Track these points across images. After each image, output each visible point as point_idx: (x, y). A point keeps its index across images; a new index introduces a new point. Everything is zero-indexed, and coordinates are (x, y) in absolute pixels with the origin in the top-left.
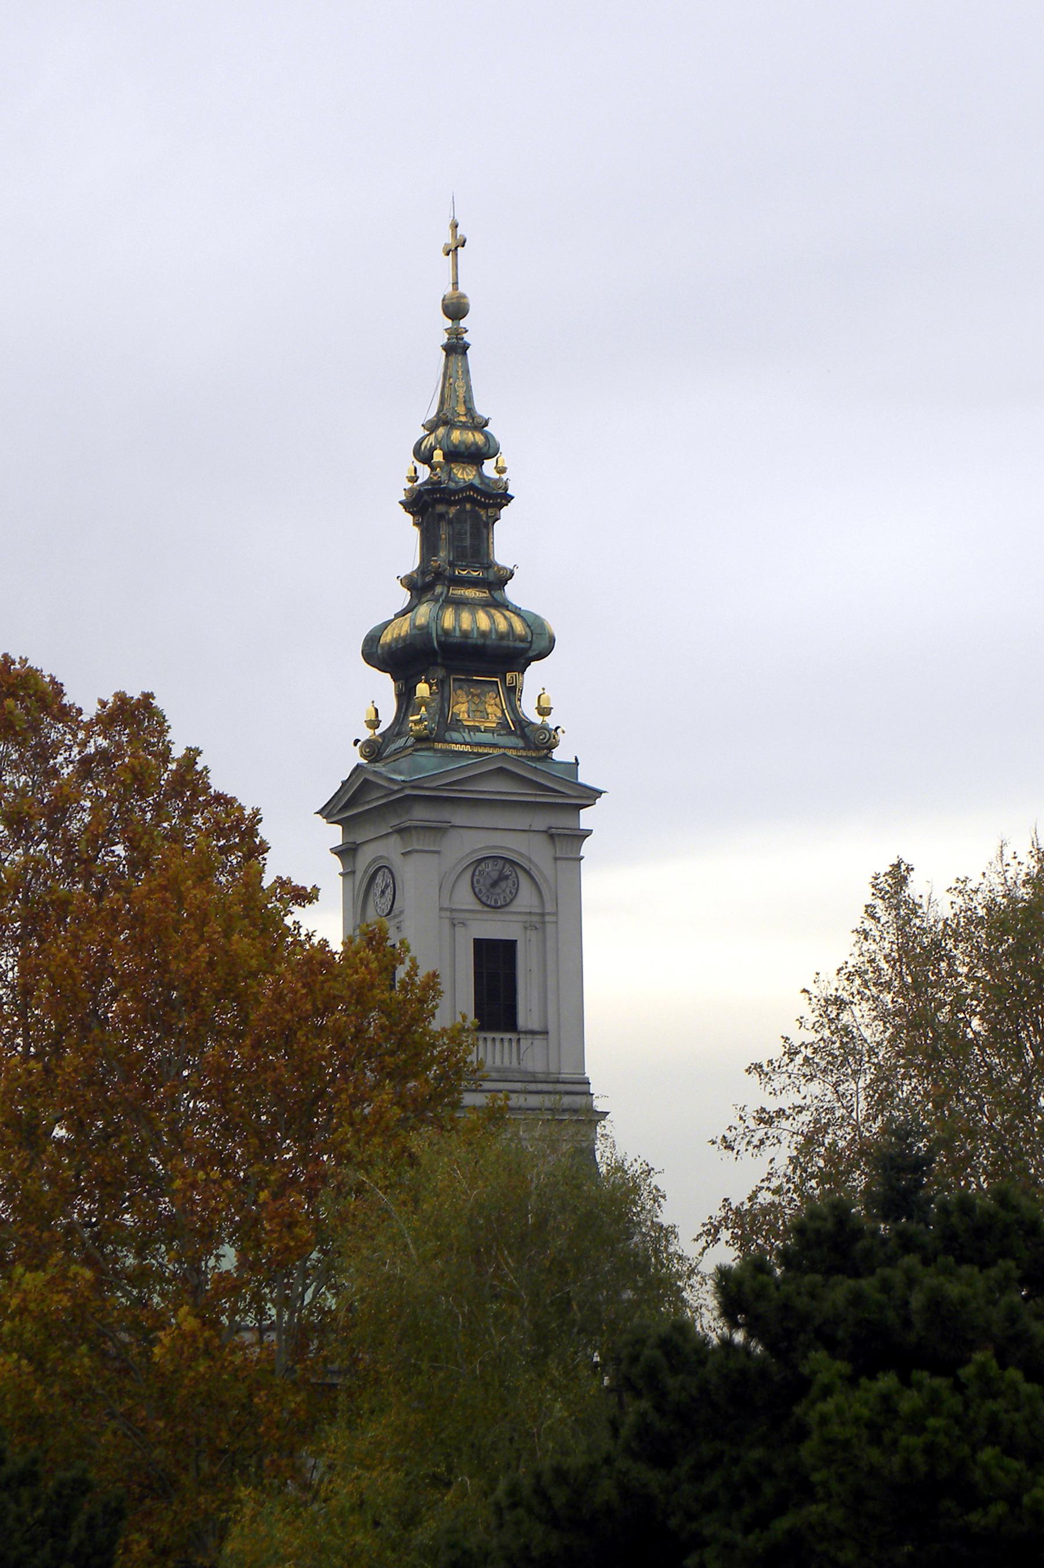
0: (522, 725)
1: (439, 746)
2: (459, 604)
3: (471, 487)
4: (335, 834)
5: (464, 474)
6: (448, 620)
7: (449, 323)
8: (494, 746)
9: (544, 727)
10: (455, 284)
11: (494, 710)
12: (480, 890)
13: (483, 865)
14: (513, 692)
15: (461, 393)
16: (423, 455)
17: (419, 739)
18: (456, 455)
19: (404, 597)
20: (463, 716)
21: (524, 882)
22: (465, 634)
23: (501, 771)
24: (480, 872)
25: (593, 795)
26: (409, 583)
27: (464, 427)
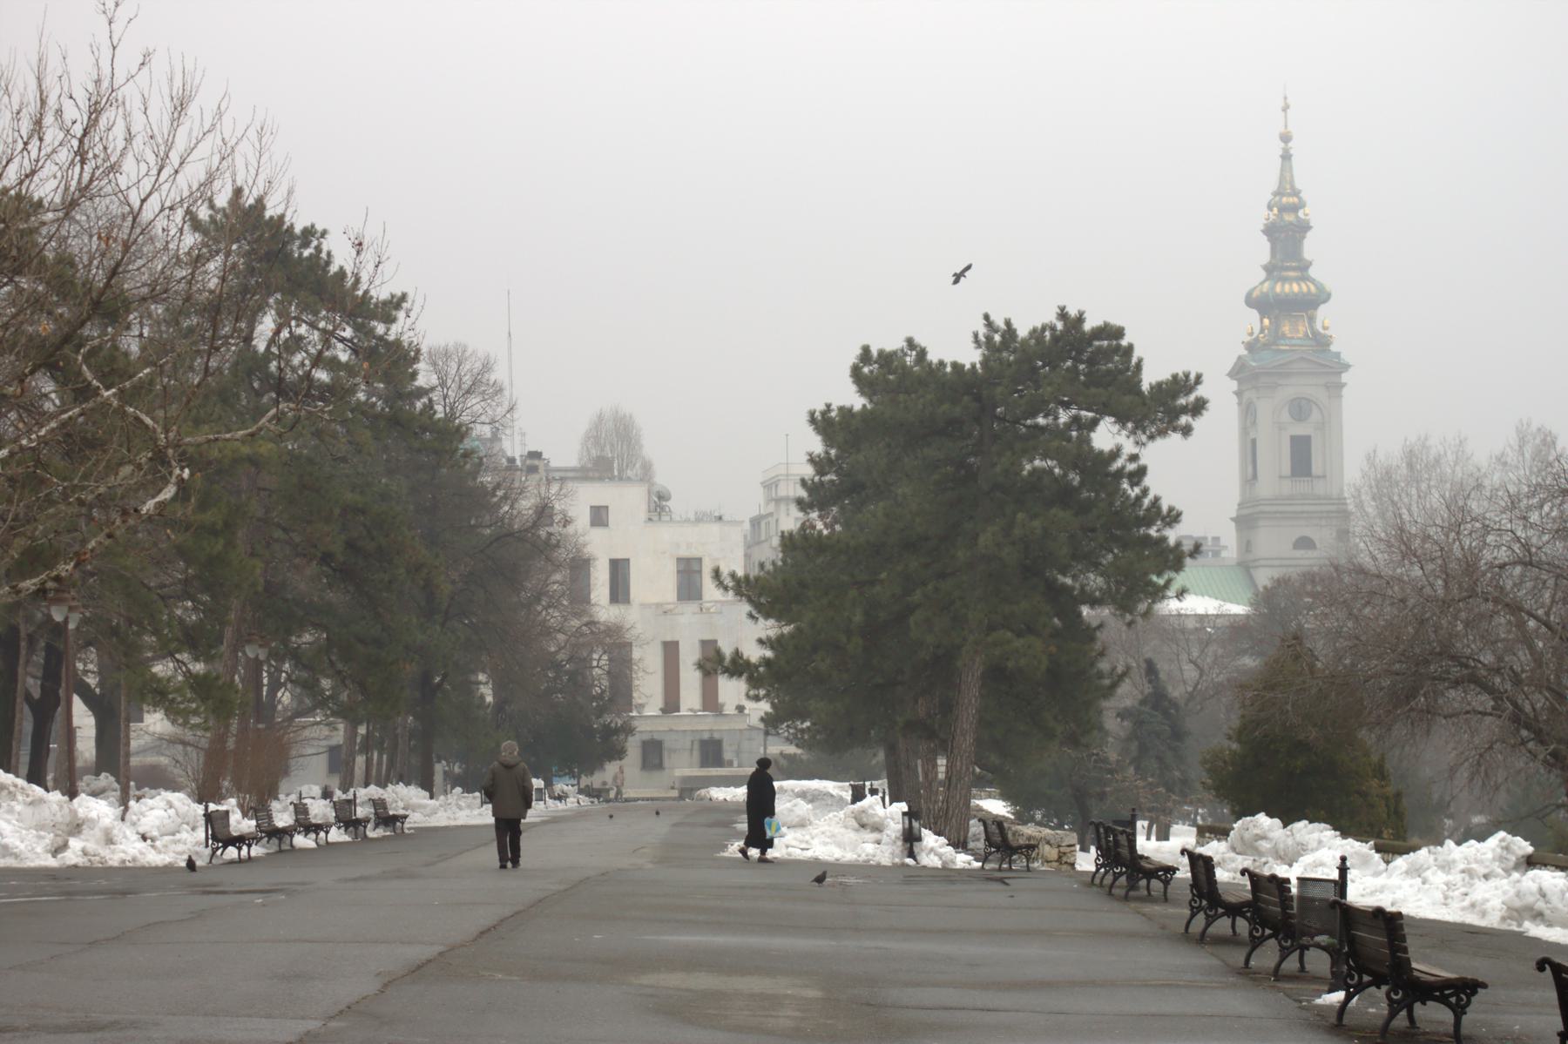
0: (1316, 334)
1: (1273, 347)
2: (1284, 280)
3: (1291, 223)
4: (1234, 385)
5: (1289, 218)
6: (1278, 289)
7: (1282, 145)
8: (1302, 346)
9: (1324, 336)
10: (1286, 126)
11: (1302, 328)
14: (1312, 319)
15: (1288, 179)
16: (1270, 208)
17: (1265, 345)
18: (1283, 209)
19: (1263, 275)
20: (1287, 332)
21: (1314, 407)
22: (1287, 295)
23: (1302, 359)
25: (1346, 367)
26: (1266, 268)
27: (1289, 195)
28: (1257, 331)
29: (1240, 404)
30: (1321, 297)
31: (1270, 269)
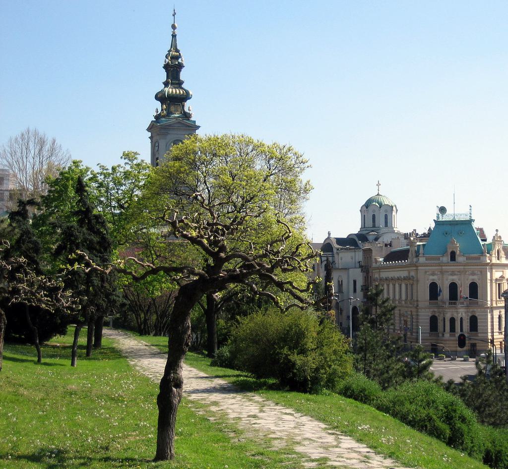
4: (149, 134)
14: (183, 106)
25: (198, 127)
28: (160, 111)
29: (152, 142)
30: (186, 97)
31: (166, 84)
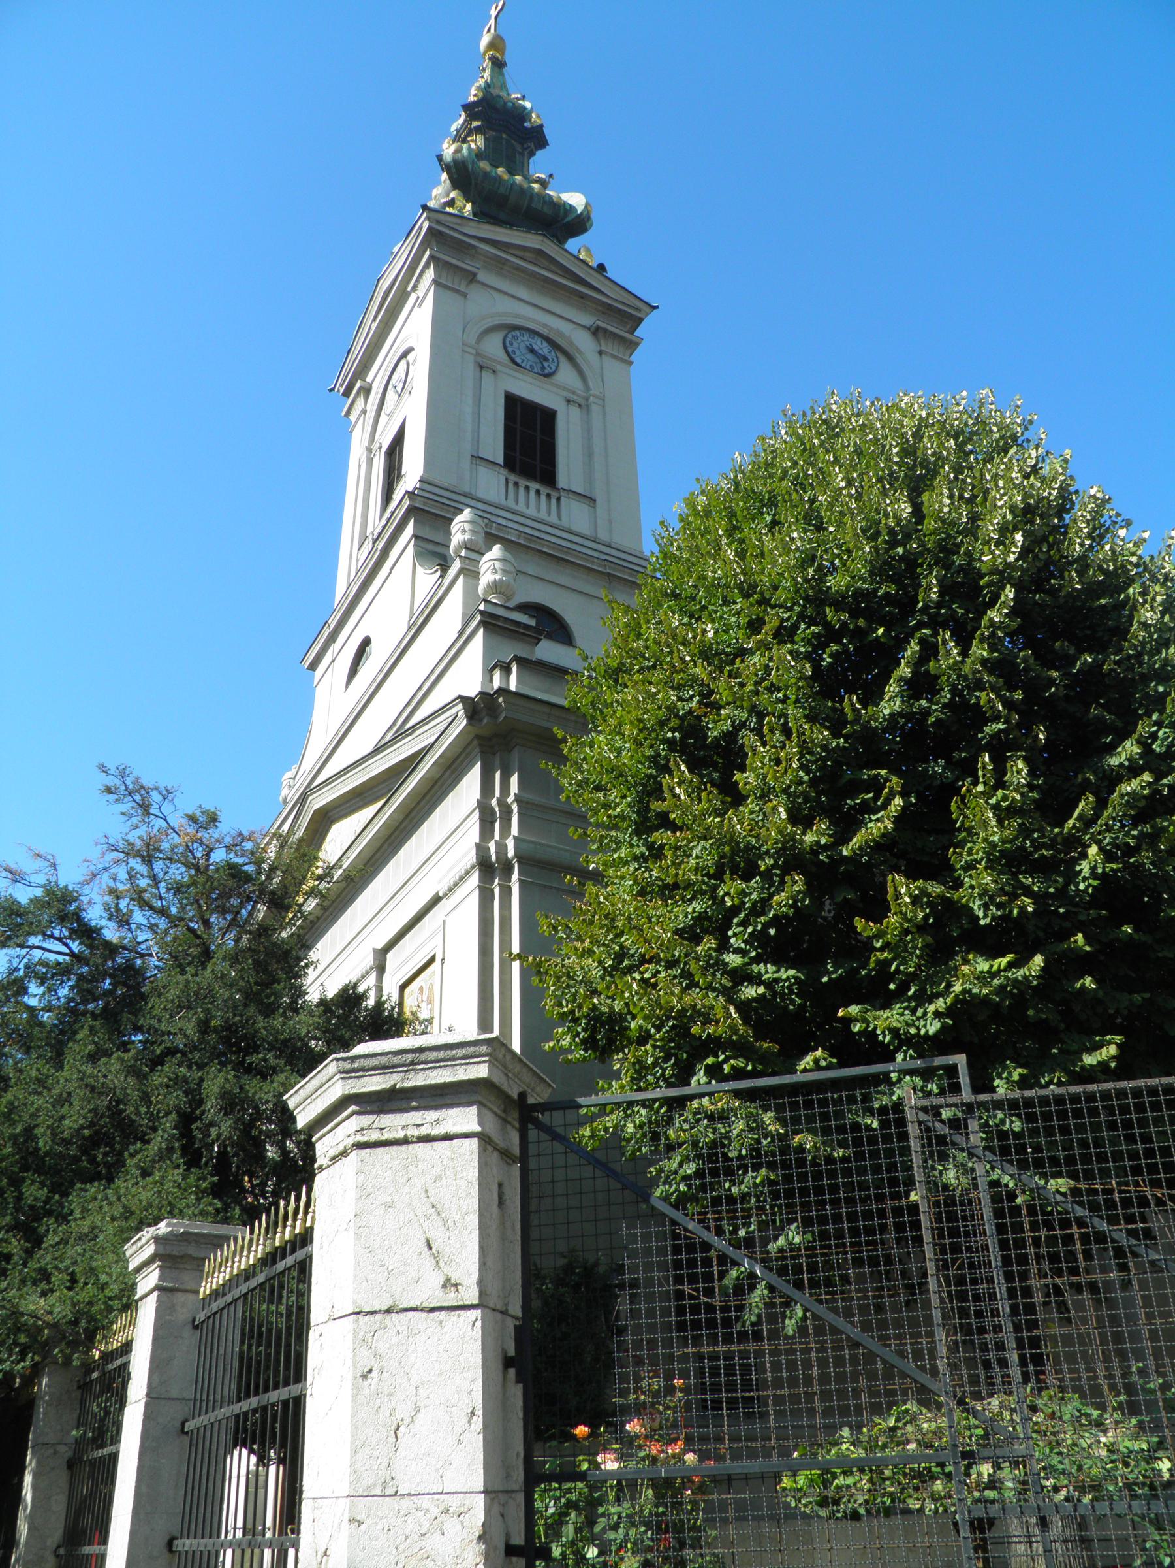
12: (513, 352)
13: (517, 333)
24: (513, 337)
